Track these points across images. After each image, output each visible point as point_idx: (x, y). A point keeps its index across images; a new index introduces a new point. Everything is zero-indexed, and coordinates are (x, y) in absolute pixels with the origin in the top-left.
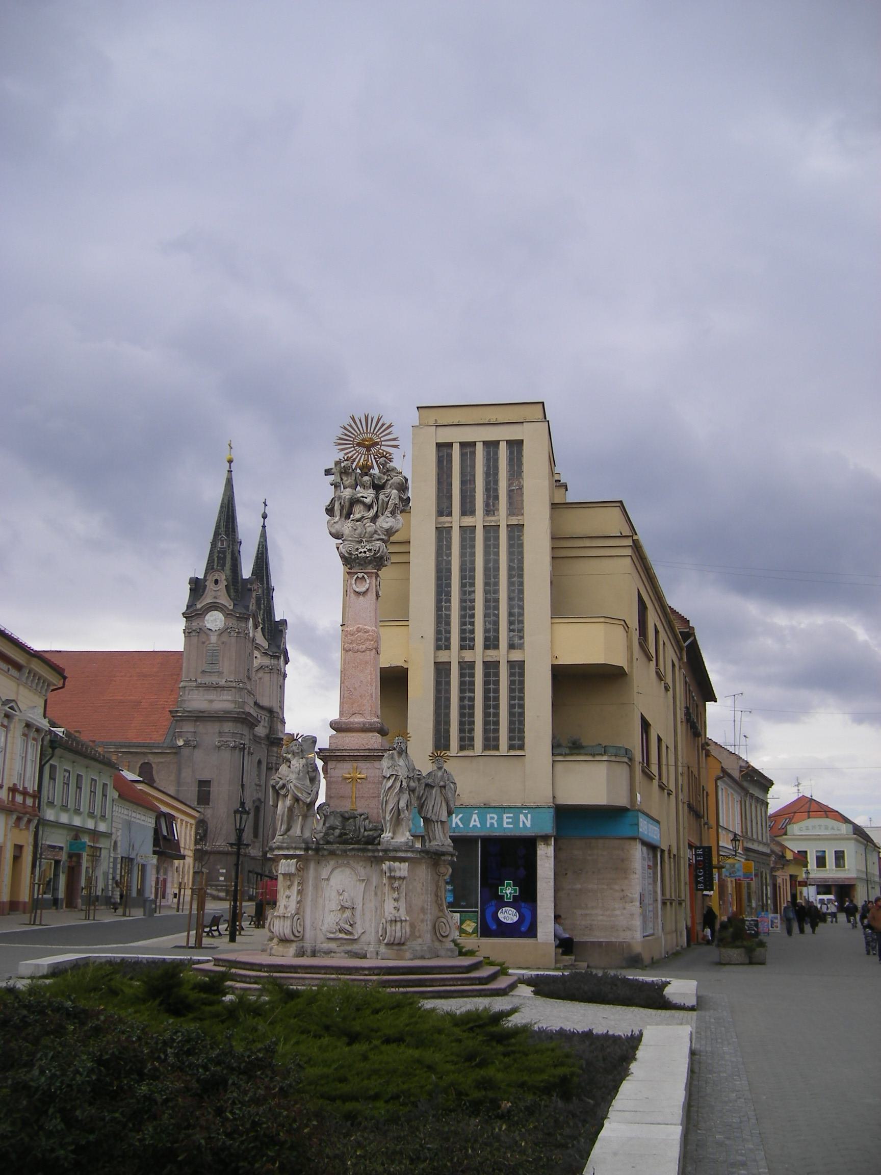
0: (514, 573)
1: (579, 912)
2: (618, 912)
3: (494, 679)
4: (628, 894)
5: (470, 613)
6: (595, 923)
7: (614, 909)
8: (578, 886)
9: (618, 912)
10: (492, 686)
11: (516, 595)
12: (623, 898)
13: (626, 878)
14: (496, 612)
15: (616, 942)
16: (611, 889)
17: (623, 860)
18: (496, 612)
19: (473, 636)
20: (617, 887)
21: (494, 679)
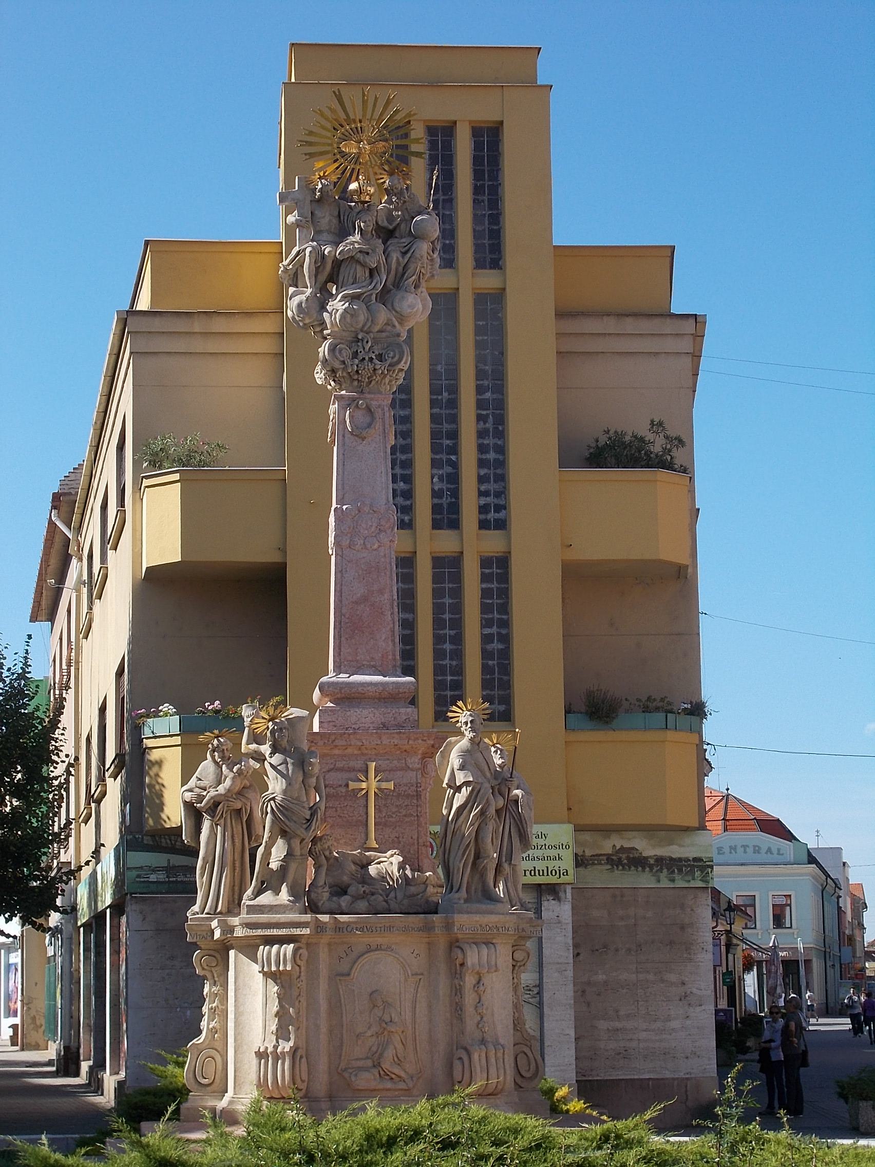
0: (486, 383)
1: (603, 1025)
2: (675, 1024)
3: (451, 586)
4: (694, 990)
5: (403, 457)
6: (634, 1044)
7: (668, 1018)
8: (601, 977)
9: (675, 1024)
10: (447, 601)
11: (489, 425)
12: (684, 997)
13: (690, 960)
14: (453, 458)
15: (674, 1079)
16: (662, 981)
17: (682, 928)
18: (453, 458)
19: (408, 503)
20: (673, 977)
21: (451, 586)
